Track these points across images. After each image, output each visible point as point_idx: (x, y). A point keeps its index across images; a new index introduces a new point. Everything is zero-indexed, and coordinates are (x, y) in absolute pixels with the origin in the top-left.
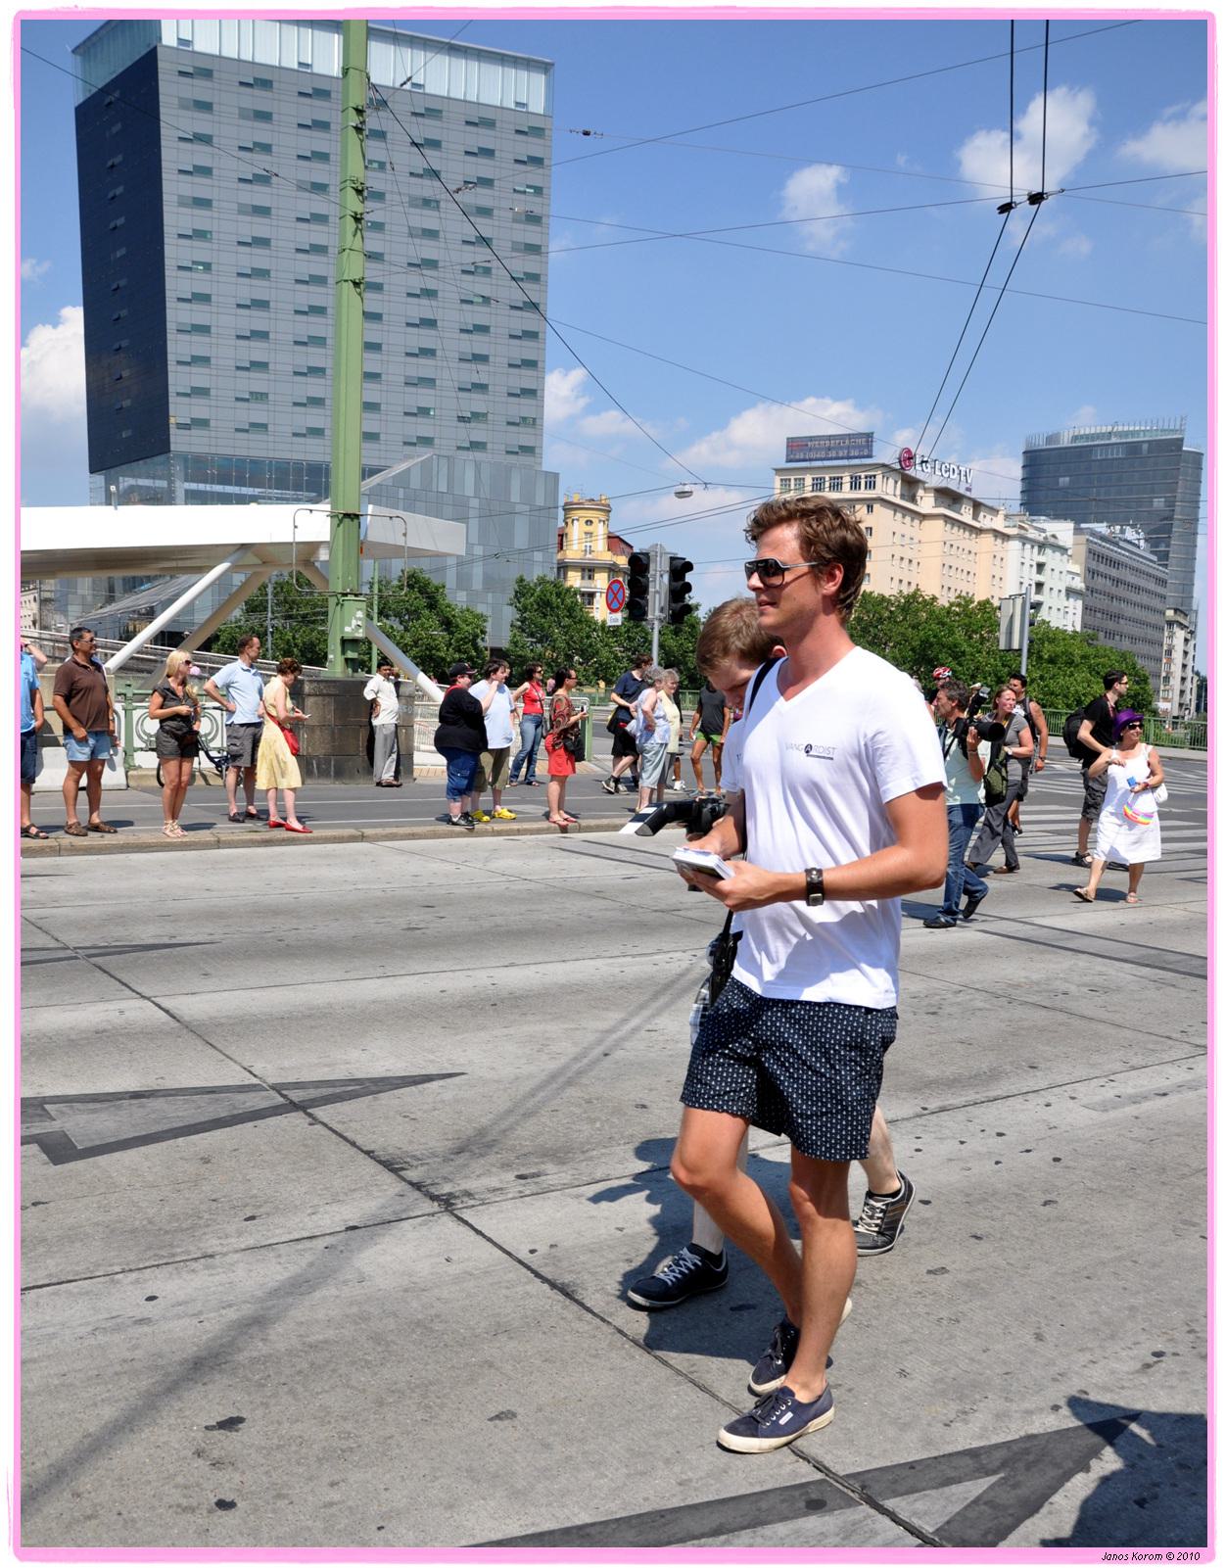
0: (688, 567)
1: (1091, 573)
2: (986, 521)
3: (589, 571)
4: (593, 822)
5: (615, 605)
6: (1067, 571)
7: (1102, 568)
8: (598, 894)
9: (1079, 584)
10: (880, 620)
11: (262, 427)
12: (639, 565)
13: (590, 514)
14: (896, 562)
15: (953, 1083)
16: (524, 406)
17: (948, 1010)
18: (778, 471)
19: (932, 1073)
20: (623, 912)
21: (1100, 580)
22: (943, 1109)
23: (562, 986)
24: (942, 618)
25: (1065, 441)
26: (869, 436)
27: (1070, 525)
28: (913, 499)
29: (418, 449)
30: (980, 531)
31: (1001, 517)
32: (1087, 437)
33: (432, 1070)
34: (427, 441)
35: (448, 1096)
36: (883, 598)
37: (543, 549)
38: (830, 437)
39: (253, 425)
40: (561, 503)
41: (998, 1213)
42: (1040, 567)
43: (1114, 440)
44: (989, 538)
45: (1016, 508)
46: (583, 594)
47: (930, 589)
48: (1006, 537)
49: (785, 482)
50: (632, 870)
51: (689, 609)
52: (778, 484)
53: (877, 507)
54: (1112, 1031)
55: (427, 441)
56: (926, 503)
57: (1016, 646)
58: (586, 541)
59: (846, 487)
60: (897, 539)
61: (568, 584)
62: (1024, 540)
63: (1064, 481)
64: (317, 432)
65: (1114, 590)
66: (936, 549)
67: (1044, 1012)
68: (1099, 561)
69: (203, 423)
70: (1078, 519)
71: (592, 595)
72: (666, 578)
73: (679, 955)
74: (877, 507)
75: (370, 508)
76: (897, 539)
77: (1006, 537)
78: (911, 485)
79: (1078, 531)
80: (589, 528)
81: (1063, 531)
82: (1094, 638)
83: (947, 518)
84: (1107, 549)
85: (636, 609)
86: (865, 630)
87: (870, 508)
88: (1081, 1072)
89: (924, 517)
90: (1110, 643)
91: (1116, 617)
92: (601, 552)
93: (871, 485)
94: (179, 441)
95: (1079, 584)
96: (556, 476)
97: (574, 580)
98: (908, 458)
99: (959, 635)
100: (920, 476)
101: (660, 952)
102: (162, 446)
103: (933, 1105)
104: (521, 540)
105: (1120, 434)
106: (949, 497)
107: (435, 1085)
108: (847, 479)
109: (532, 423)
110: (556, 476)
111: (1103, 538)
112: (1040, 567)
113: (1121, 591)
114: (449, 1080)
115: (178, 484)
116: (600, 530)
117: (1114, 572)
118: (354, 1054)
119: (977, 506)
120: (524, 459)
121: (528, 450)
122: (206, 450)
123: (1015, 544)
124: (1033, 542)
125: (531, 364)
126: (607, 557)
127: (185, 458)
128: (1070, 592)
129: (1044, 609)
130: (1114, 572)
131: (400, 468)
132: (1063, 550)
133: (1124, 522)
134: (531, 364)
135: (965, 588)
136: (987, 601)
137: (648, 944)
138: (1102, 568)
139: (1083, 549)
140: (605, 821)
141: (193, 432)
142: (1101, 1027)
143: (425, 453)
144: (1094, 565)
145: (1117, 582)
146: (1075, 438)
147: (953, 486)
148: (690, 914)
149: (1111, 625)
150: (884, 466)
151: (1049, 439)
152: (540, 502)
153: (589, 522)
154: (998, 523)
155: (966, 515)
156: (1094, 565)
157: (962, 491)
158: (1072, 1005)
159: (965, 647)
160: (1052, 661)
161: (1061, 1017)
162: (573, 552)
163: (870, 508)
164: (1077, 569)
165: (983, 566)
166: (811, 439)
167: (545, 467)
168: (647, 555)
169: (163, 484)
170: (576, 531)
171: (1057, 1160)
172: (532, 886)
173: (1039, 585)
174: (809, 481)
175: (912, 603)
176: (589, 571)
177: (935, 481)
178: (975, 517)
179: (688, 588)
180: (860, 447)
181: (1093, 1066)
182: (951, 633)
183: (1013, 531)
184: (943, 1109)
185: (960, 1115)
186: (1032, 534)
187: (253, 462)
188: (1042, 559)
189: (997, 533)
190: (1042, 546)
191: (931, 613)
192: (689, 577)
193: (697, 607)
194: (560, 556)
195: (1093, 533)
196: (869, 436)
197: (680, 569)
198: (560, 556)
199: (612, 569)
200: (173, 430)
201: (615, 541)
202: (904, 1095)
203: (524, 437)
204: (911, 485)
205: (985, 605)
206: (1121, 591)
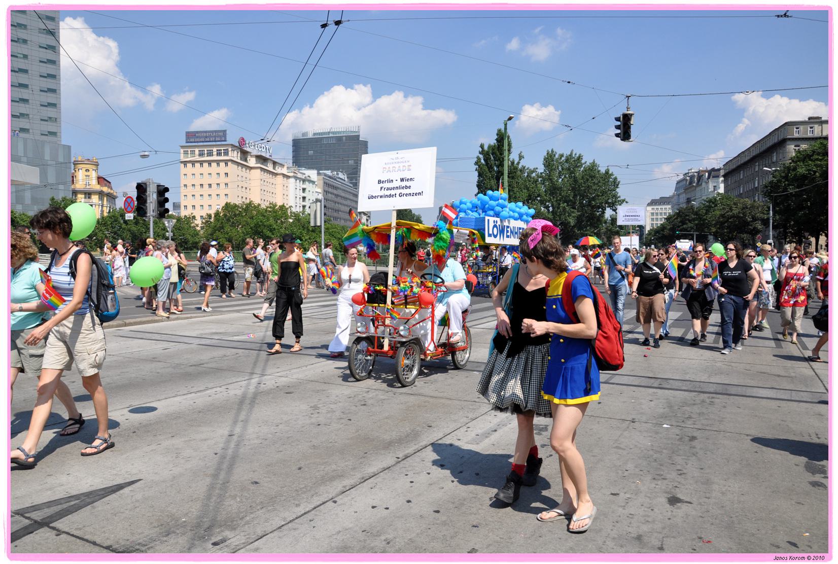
0: (167, 190)
1: (326, 192)
2: (279, 170)
4: (132, 321)
5: (129, 209)
6: (315, 192)
7: (330, 190)
8: (154, 359)
9: (320, 197)
10: (235, 215)
12: (141, 189)
13: (88, 167)
14: (240, 189)
15: (401, 441)
16: (51, 112)
17: (370, 402)
18: (182, 147)
19: (387, 437)
20: (174, 368)
21: (330, 195)
22: (406, 457)
23: (167, 416)
24: (263, 213)
25: (310, 136)
26: (225, 131)
27: (315, 172)
28: (246, 160)
30: (276, 174)
31: (285, 168)
32: (319, 134)
33: (120, 481)
35: (139, 496)
36: (236, 205)
37: (64, 183)
38: (206, 132)
40: (73, 159)
41: (474, 510)
42: (304, 190)
43: (331, 135)
44: (280, 178)
45: (291, 165)
47: (256, 201)
48: (288, 177)
49: (186, 153)
50: (165, 345)
51: (167, 211)
52: (182, 151)
53: (229, 163)
54: (450, 402)
56: (252, 162)
57: (318, 224)
59: (215, 153)
60: (239, 178)
62: (296, 178)
63: (311, 152)
65: (336, 199)
66: (258, 183)
67: (412, 397)
68: (329, 186)
70: (319, 169)
72: (155, 196)
73: (218, 389)
74: (229, 163)
76: (239, 178)
77: (288, 177)
78: (245, 154)
79: (319, 174)
80: (87, 173)
81: (312, 174)
82: (330, 220)
83: (261, 168)
84: (331, 182)
85: (141, 210)
86: (228, 220)
87: (226, 164)
88: (453, 426)
89: (251, 168)
90: (336, 223)
91: (337, 211)
92: (94, 185)
93: (226, 153)
95: (320, 197)
96: (69, 147)
98: (242, 141)
99: (272, 221)
100: (248, 149)
101: (207, 389)
103: (401, 455)
104: (51, 179)
105: (333, 133)
106: (262, 159)
107: (126, 490)
108: (215, 149)
109: (54, 120)
110: (69, 147)
111: (330, 177)
112: (304, 190)
113: (339, 200)
114: (134, 486)
116: (94, 175)
117: (335, 192)
118: (63, 479)
119: (275, 163)
121: (54, 134)
123: (292, 180)
124: (300, 179)
125: (53, 91)
126: (98, 187)
128: (317, 200)
129: (307, 208)
130: (335, 192)
132: (313, 182)
133: (337, 170)
134: (53, 91)
135: (273, 200)
136: (283, 205)
137: (200, 385)
138: (330, 190)
139: (322, 182)
140: (139, 320)
142: (443, 401)
144: (327, 189)
145: (337, 196)
146: (315, 134)
147: (264, 154)
148: (209, 365)
149: (335, 214)
150: (232, 145)
151: (304, 134)
152: (61, 159)
153: (87, 170)
154: (284, 171)
155: (270, 167)
156: (327, 189)
157: (268, 156)
158: (422, 391)
159: (275, 226)
160: (313, 231)
161: (423, 398)
162: (80, 185)
163: (226, 164)
164: (319, 190)
165: (279, 190)
166: (197, 132)
167: (63, 143)
168: (145, 184)
170: (81, 175)
171: (477, 474)
172: (115, 358)
173: (304, 198)
174: (197, 152)
175: (249, 207)
177: (255, 153)
178: (274, 168)
179: (167, 200)
180: (220, 137)
181: (455, 421)
182: (268, 220)
183: (291, 174)
184: (406, 457)
185: (416, 458)
186: (299, 175)
188: (304, 186)
189: (284, 175)
190: (304, 181)
191: (258, 211)
192: (167, 195)
194: (73, 187)
195: (325, 175)
196: (225, 131)
197: (162, 191)
198: (73, 187)
199: (101, 194)
201: (101, 180)
202: (383, 452)
203: (51, 127)
204: (245, 154)
205: (282, 207)
206: (339, 200)
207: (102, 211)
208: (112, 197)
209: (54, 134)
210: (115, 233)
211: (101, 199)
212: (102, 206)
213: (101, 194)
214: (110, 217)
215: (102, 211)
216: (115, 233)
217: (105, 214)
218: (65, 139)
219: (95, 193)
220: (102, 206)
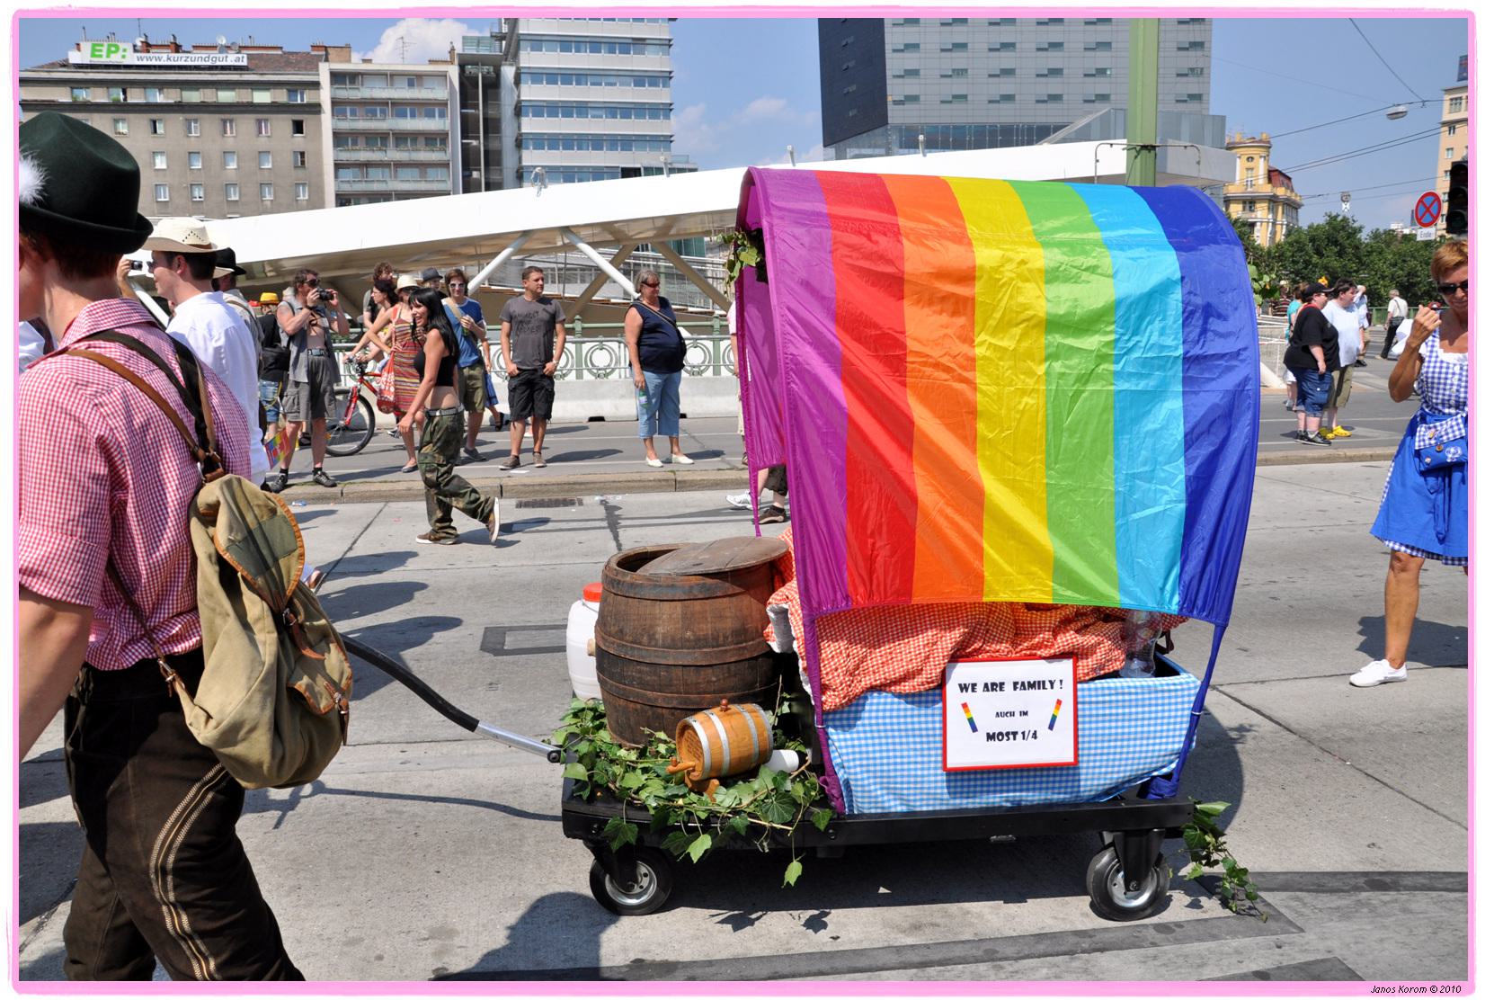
3: (1250, 203)
11: (965, 97)
13: (1251, 152)
29: (1097, 105)
34: (1103, 98)
39: (955, 97)
40: (1227, 140)
46: (1245, 224)
55: (1103, 98)
58: (1247, 175)
61: (1234, 216)
64: (1009, 98)
69: (913, 99)
71: (1253, 225)
75: (1170, 142)
80: (1250, 164)
94: (896, 115)
96: (1223, 118)
97: (1236, 211)
102: (883, 120)
110: (1223, 118)
115: (896, 149)
116: (1261, 168)
120: (1193, 106)
121: (1197, 97)
122: (915, 121)
126: (1267, 189)
127: (899, 128)
131: (1084, 121)
141: (907, 106)
143: (1103, 108)
153: (1250, 159)
169: (883, 151)
176: (1250, 203)
187: (955, 128)
193: (1360, 229)
199: (1273, 201)
200: (890, 107)
201: (1273, 175)
207: (1274, 233)
208: (1292, 206)
209: (1197, 97)
210: (1297, 273)
211: (1272, 210)
212: (1274, 224)
213: (1273, 201)
214: (1291, 244)
215: (1274, 233)
216: (1297, 273)
217: (1280, 237)
218: (1215, 108)
219: (1262, 199)
220: (1274, 224)
